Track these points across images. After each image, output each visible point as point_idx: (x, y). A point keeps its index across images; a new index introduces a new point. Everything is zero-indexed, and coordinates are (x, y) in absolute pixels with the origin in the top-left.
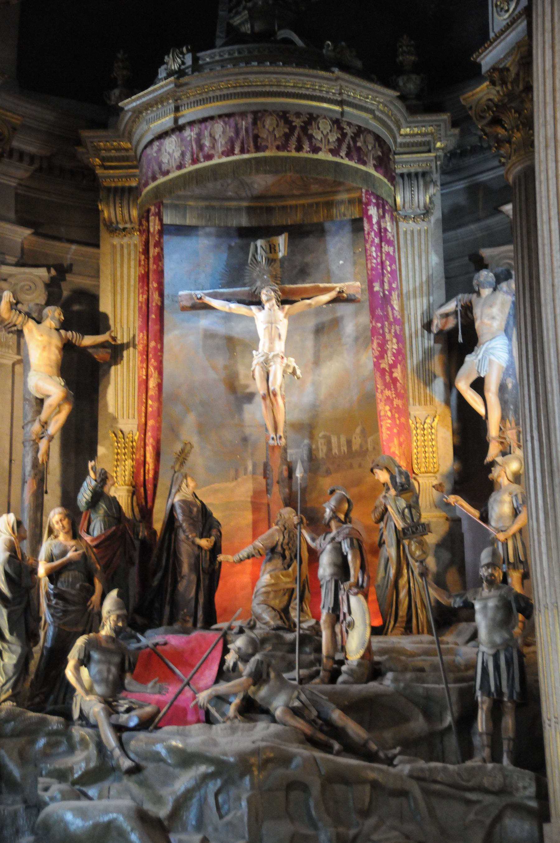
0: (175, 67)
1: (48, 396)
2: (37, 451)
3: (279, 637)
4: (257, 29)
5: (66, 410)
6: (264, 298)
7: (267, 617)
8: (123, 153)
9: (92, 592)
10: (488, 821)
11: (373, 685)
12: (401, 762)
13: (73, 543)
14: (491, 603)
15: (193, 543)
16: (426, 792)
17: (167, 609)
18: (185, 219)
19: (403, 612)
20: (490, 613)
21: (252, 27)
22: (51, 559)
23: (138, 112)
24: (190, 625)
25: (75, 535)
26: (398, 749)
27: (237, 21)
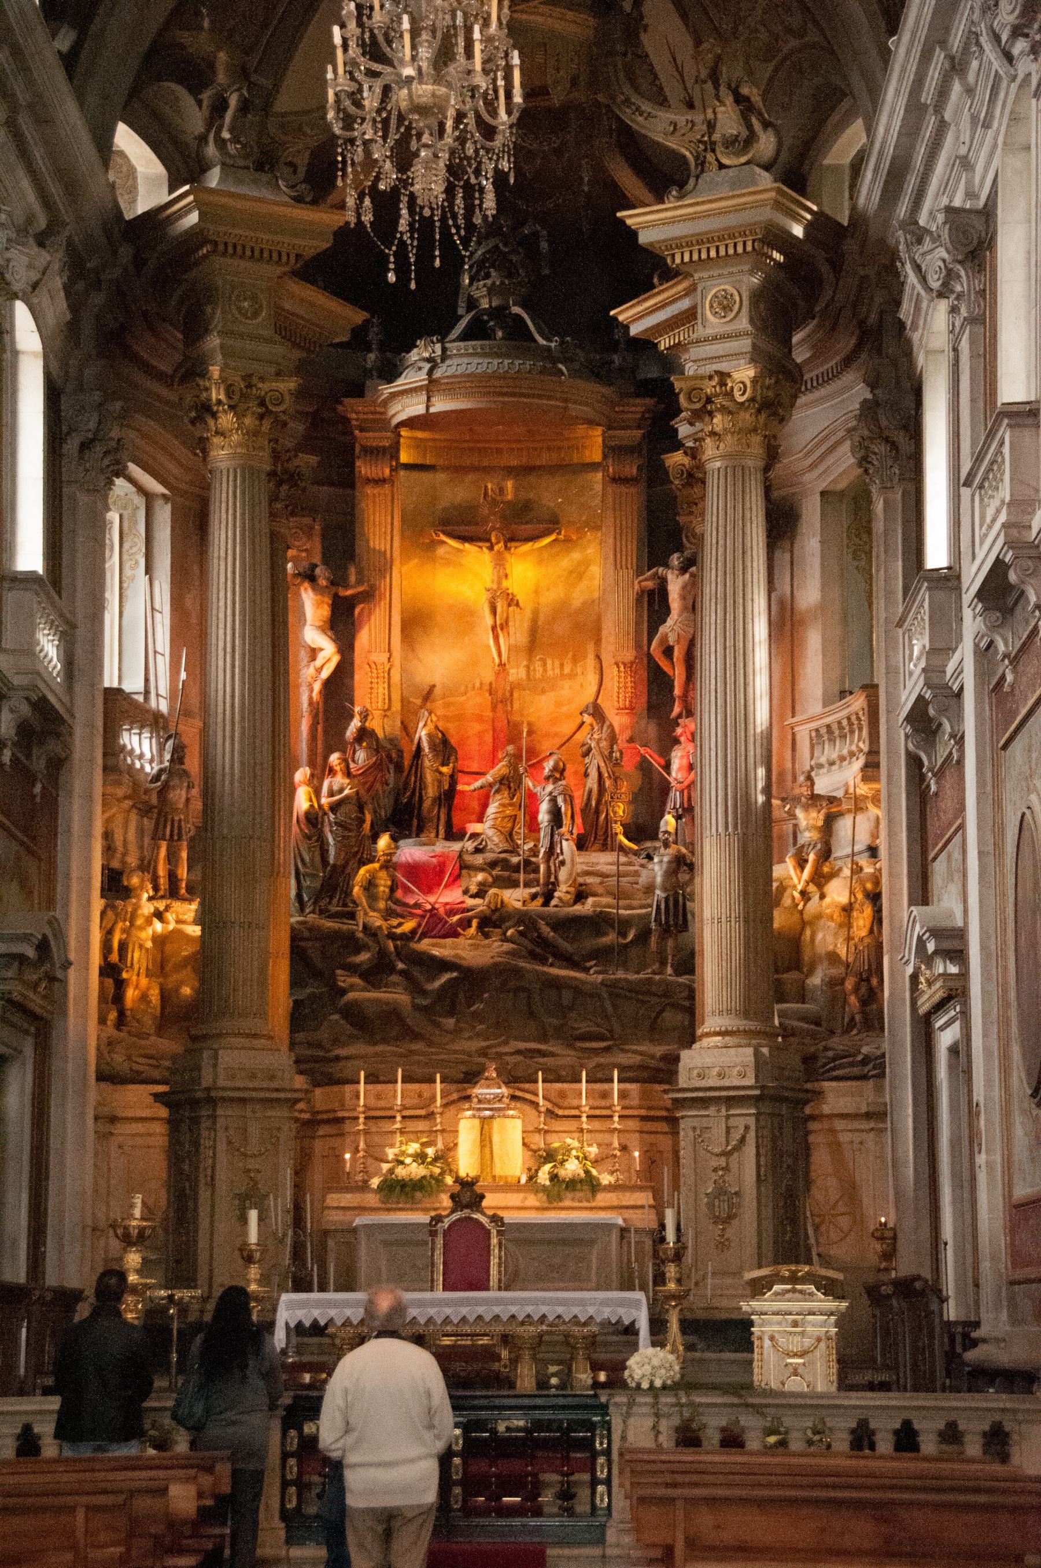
0: (426, 355)
1: (321, 650)
2: (312, 690)
3: (505, 861)
4: (494, 304)
5: (336, 659)
6: (493, 539)
7: (496, 839)
8: (378, 416)
9: (362, 821)
10: (654, 1015)
11: (578, 907)
12: (596, 972)
13: (347, 781)
14: (666, 859)
15: (437, 771)
16: (611, 995)
17: (415, 822)
18: (425, 455)
19: (600, 833)
20: (665, 866)
21: (490, 302)
22: (331, 794)
23: (394, 396)
24: (433, 835)
25: (348, 774)
26: (593, 962)
27: (476, 294)
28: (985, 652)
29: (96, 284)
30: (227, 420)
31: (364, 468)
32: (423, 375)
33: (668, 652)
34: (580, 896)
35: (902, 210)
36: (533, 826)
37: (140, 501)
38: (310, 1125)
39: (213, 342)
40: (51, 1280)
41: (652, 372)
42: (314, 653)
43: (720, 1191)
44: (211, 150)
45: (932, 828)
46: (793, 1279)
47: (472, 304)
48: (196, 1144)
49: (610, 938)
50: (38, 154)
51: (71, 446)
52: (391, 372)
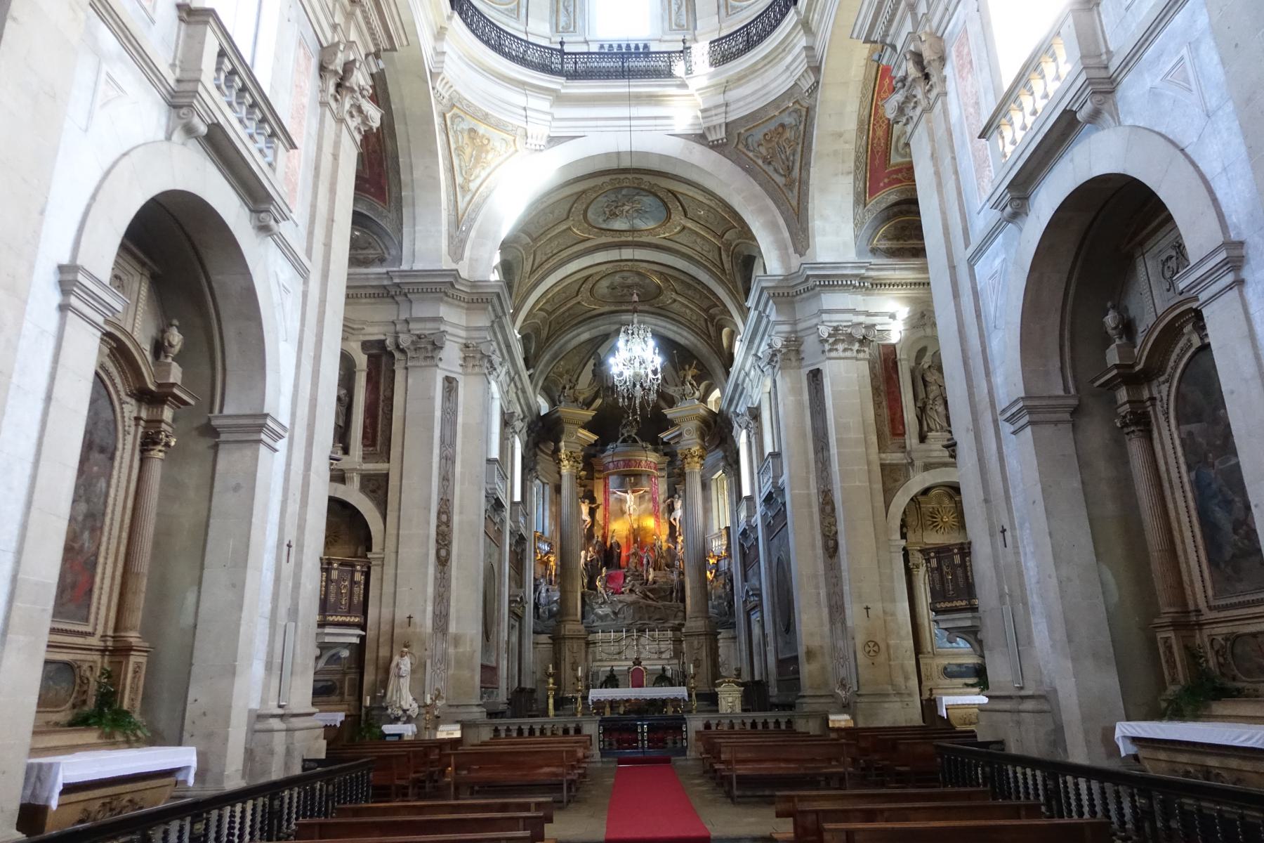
28: (764, 517)
29: (533, 432)
30: (566, 463)
31: (597, 475)
32: (611, 452)
33: (675, 519)
34: (655, 582)
35: (732, 409)
36: (642, 565)
37: (541, 484)
38: (588, 644)
39: (562, 444)
40: (523, 686)
41: (667, 450)
42: (585, 521)
43: (697, 659)
44: (562, 398)
45: (748, 563)
46: (729, 682)
47: (623, 435)
48: (560, 649)
49: (663, 594)
50: (522, 401)
51: (526, 471)
52: (603, 452)
